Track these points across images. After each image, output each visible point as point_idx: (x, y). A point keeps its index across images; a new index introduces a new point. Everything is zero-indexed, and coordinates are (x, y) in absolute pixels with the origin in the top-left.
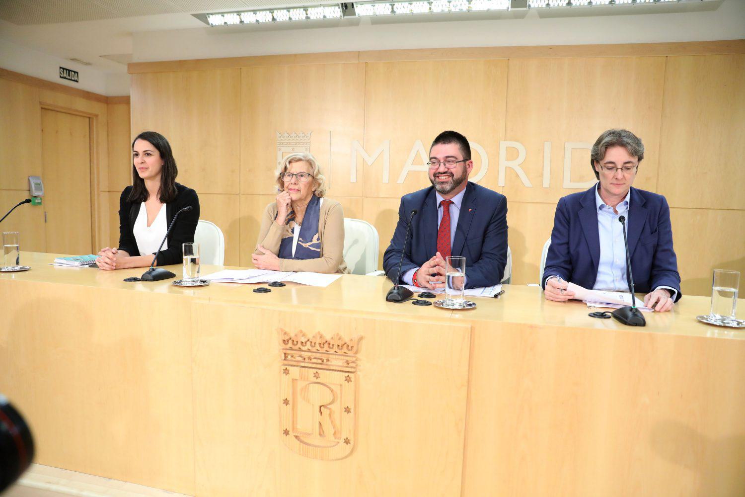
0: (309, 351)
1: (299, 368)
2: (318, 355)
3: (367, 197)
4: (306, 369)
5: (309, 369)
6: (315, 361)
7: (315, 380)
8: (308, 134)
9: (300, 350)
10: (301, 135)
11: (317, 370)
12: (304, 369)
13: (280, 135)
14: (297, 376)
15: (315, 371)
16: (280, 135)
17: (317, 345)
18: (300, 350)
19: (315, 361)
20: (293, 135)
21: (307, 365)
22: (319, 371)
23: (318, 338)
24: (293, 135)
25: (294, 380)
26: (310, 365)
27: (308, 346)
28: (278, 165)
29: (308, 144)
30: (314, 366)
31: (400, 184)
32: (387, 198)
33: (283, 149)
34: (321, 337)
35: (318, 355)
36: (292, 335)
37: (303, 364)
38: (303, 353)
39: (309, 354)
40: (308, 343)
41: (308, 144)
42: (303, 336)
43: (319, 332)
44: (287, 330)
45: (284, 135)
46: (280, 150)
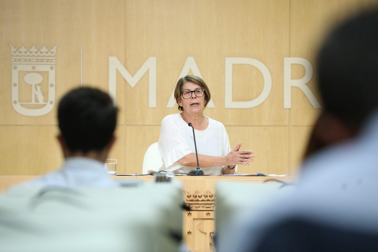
0: (203, 200)
1: (197, 212)
2: (209, 202)
3: (129, 125)
4: (202, 212)
5: (204, 212)
6: (207, 206)
7: (207, 217)
8: (52, 48)
9: (197, 200)
10: (44, 50)
11: (209, 212)
12: (200, 212)
13: (15, 50)
14: (197, 218)
15: (207, 212)
16: (15, 50)
17: (208, 196)
18: (197, 200)
19: (207, 206)
20: (34, 49)
21: (202, 209)
22: (210, 212)
23: (209, 192)
24: (34, 49)
25: (194, 219)
26: (204, 209)
27: (203, 198)
28: (13, 87)
29: (53, 61)
30: (207, 209)
31: (170, 108)
32: (154, 125)
33: (20, 67)
34: (210, 192)
35: (209, 202)
36: (192, 194)
37: (199, 209)
38: (200, 202)
39: (204, 202)
40: (203, 196)
41: (53, 61)
42: (199, 193)
43: (208, 190)
44: (189, 191)
45: (20, 50)
46: (15, 68)
